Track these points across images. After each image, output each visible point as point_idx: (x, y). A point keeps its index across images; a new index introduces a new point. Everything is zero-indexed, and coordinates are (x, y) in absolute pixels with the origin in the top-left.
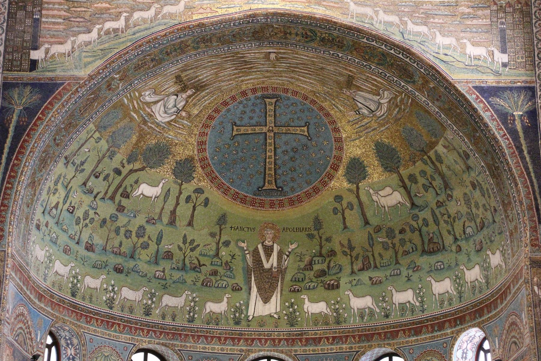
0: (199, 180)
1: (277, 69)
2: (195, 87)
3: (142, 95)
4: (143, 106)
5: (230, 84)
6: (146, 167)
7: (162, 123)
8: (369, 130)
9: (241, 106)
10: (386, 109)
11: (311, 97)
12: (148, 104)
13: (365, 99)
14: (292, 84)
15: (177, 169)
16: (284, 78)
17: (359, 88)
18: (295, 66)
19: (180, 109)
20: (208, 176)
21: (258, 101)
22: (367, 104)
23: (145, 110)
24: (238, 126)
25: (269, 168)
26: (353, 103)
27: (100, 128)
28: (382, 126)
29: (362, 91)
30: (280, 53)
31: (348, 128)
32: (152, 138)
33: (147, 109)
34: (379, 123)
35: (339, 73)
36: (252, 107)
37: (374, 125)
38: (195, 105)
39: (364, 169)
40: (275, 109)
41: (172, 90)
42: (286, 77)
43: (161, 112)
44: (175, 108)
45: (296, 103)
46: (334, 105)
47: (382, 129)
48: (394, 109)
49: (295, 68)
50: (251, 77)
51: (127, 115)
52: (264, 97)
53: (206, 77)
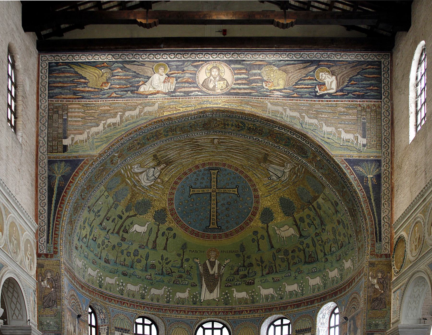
0: (170, 223)
1: (219, 150)
2: (165, 163)
3: (132, 168)
4: (133, 175)
5: (188, 161)
6: (137, 215)
7: (146, 186)
8: (277, 190)
9: (195, 175)
10: (288, 176)
11: (240, 168)
12: (137, 174)
13: (275, 169)
14: (228, 160)
15: (156, 216)
16: (223, 156)
17: (271, 162)
18: (230, 148)
19: (157, 177)
20: (175, 220)
21: (206, 172)
22: (276, 173)
23: (135, 178)
24: (193, 189)
25: (213, 215)
26: (267, 172)
27: (108, 189)
28: (285, 187)
29: (273, 164)
30: (221, 139)
31: (263, 189)
32: (140, 196)
33: (136, 177)
34: (283, 185)
35: (259, 152)
36: (202, 176)
37: (280, 186)
38: (166, 174)
39: (272, 215)
40: (217, 177)
41: (151, 164)
42: (224, 155)
43: (145, 180)
44: (154, 177)
45: (230, 173)
46: (255, 174)
47: (284, 189)
48: (293, 176)
49: (230, 149)
50: (202, 156)
51: (124, 181)
52: (210, 169)
53: (172, 156)
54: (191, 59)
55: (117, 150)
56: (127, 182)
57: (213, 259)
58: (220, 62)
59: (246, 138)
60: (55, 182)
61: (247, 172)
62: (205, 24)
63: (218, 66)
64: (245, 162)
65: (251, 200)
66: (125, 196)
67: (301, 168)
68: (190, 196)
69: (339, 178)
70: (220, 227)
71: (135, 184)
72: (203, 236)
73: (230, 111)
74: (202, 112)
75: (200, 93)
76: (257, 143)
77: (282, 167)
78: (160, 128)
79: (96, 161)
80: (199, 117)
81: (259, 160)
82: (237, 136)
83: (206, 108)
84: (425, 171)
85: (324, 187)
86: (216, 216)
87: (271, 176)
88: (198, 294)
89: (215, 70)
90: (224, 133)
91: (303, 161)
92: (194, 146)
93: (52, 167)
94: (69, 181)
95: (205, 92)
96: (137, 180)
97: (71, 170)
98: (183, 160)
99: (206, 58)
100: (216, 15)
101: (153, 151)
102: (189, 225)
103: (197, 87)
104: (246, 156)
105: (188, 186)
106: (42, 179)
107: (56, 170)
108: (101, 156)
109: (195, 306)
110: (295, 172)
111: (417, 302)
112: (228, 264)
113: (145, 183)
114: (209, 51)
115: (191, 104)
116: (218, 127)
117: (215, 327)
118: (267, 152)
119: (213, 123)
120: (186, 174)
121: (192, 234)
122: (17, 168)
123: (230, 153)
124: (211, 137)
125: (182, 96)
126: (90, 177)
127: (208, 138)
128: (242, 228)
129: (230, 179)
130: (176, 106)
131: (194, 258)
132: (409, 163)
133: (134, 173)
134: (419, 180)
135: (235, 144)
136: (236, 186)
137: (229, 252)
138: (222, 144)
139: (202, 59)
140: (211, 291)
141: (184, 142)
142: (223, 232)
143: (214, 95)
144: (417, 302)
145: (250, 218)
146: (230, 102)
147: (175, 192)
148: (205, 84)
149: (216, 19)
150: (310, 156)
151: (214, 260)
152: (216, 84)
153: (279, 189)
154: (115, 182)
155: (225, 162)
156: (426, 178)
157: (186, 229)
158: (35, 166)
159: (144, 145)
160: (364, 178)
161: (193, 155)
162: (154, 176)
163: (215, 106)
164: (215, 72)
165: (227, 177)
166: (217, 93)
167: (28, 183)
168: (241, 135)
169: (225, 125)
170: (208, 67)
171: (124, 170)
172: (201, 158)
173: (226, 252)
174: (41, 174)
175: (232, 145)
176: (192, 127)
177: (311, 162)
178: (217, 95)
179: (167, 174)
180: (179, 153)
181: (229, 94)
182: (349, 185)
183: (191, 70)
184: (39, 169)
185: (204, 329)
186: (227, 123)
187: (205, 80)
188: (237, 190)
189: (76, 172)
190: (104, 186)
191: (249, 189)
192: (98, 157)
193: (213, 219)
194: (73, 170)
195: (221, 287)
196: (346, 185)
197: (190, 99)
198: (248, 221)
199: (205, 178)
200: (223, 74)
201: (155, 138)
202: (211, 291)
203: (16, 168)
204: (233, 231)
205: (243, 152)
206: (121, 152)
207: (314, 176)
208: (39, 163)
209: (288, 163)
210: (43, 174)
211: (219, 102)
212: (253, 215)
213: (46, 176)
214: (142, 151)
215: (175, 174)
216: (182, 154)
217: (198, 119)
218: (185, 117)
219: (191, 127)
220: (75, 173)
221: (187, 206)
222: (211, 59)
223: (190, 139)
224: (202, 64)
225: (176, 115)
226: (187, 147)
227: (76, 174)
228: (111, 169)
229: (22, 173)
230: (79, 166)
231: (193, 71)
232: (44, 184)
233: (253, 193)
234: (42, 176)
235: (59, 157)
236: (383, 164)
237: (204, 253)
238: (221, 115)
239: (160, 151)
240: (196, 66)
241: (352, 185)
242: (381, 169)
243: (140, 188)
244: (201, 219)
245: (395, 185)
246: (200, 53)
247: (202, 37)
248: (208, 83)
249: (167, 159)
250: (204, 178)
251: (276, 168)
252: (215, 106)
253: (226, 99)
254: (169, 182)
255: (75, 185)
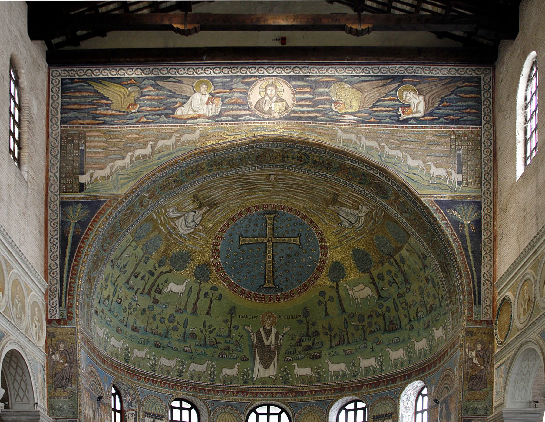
1: (276, 189)
2: (209, 205)
3: (167, 212)
4: (168, 220)
5: (237, 202)
8: (349, 239)
9: (246, 221)
10: (363, 221)
11: (303, 212)
12: (172, 219)
13: (347, 213)
14: (288, 201)
16: (281, 197)
17: (342, 205)
18: (291, 186)
19: (198, 223)
20: (220, 277)
21: (260, 217)
22: (348, 218)
23: (170, 224)
24: (244, 237)
25: (268, 270)
26: (337, 217)
27: (136, 238)
28: (359, 236)
29: (345, 207)
31: (332, 238)
33: (172, 223)
34: (357, 233)
35: (327, 192)
36: (255, 222)
37: (353, 235)
38: (209, 220)
40: (273, 223)
41: (191, 207)
42: (283, 196)
43: (183, 226)
44: (194, 223)
45: (290, 218)
46: (321, 219)
47: (359, 238)
48: (370, 221)
49: (291, 187)
50: (255, 196)
51: (156, 228)
52: (265, 213)
53: (218, 196)
54: (240, 74)
55: (147, 188)
56: (161, 229)
57: (268, 326)
58: (277, 78)
59: (310, 174)
60: (70, 229)
61: (312, 216)
62: (259, 31)
63: (275, 83)
64: (309, 204)
65: (317, 252)
66: (158, 247)
67: (380, 212)
68: (240, 247)
69: (427, 224)
70: (277, 286)
71: (170, 231)
72: (256, 298)
73: (290, 140)
74: (254, 141)
75: (252, 118)
76: (324, 181)
77: (356, 210)
78: (202, 161)
79: (121, 203)
80: (251, 147)
81: (326, 201)
82: (299, 171)
83: (260, 136)
84: (536, 215)
85: (409, 236)
86: (273, 272)
87: (342, 222)
88: (250, 370)
89: (271, 88)
90: (283, 168)
91: (382, 203)
92: (245, 184)
93: (66, 211)
94: (87, 228)
95: (259, 116)
96: (173, 227)
97: (89, 214)
98: (231, 202)
99: (260, 73)
100: (272, 18)
101: (193, 190)
102: (239, 284)
103: (248, 110)
104: (311, 196)
105: (237, 234)
106: (53, 225)
107: (71, 214)
108: (127, 197)
109: (246, 385)
110: (372, 217)
111: (526, 380)
112: (288, 333)
113: (183, 230)
114: (264, 65)
115: (241, 132)
116: (275, 160)
117: (271, 412)
118: (337, 191)
119: (268, 155)
120: (234, 220)
121: (242, 295)
122: (22, 211)
123: (290, 192)
124: (267, 173)
125: (229, 121)
126: (113, 223)
127: (263, 173)
128: (305, 287)
129: (290, 226)
130: (222, 133)
131: (245, 325)
132: (516, 205)
133: (169, 218)
134: (529, 227)
135: (297, 182)
136: (298, 235)
137: (288, 317)
138: (280, 181)
139: (255, 74)
140: (266, 367)
141: (232, 179)
142: (281, 292)
143: (270, 120)
144: (526, 380)
145: (316, 275)
146: (290, 129)
147: (221, 241)
148: (258, 106)
149: (273, 24)
150: (391, 197)
151: (270, 327)
152: (273, 106)
153: (352, 239)
154: (145, 229)
155: (284, 204)
156: (537, 224)
157: (235, 288)
158: (44, 209)
159: (181, 182)
160: (459, 225)
161: (243, 195)
162: (194, 221)
163: (271, 134)
164: (271, 91)
165: (286, 222)
166: (274, 117)
167: (35, 230)
168: (304, 171)
169: (284, 157)
170: (263, 84)
171: (156, 214)
172: (254, 200)
173: (285, 317)
174: (51, 219)
175: (293, 182)
176: (243, 160)
177: (392, 204)
178: (274, 120)
179: (210, 219)
180: (226, 193)
181: (288, 118)
182: (440, 233)
183: (241, 88)
184: (49, 213)
185: (258, 415)
186: (286, 155)
187: (259, 100)
188: (300, 239)
189: (96, 217)
190: (131, 234)
191: (315, 238)
192: (124, 198)
193: (269, 276)
194: (92, 214)
195: (279, 361)
196: (436, 233)
197: (239, 125)
198: (313, 279)
199: (259, 224)
200: (282, 93)
201: (195, 173)
202: (266, 367)
203: (20, 212)
204: (294, 291)
205: (306, 191)
206: (153, 191)
207: (396, 222)
208: (49, 205)
209: (364, 205)
210: (54, 220)
211: (277, 128)
212: (319, 271)
213: (58, 222)
214: (179, 190)
215: (220, 219)
216: (230, 194)
217: (250, 150)
218: (234, 147)
219: (241, 160)
220: (95, 218)
221: (236, 260)
222: (266, 74)
223: (240, 175)
224: (255, 81)
225: (222, 145)
226: (236, 185)
227: (96, 219)
228: (140, 213)
229: (28, 218)
230: (99, 209)
231: (244, 89)
232: (56, 232)
233: (319, 243)
234: (53, 222)
235: (74, 198)
236: (483, 206)
237: (258, 319)
238: (279, 145)
239: (202, 191)
240: (247, 84)
241: (444, 232)
242: (480, 213)
243: (176, 237)
244: (254, 276)
245: (499, 233)
246: (253, 67)
247: (255, 47)
248: (262, 104)
249: (210, 200)
250: (257, 224)
251: (348, 211)
252: (271, 133)
253: (285, 125)
254: (213, 230)
255: (94, 233)
